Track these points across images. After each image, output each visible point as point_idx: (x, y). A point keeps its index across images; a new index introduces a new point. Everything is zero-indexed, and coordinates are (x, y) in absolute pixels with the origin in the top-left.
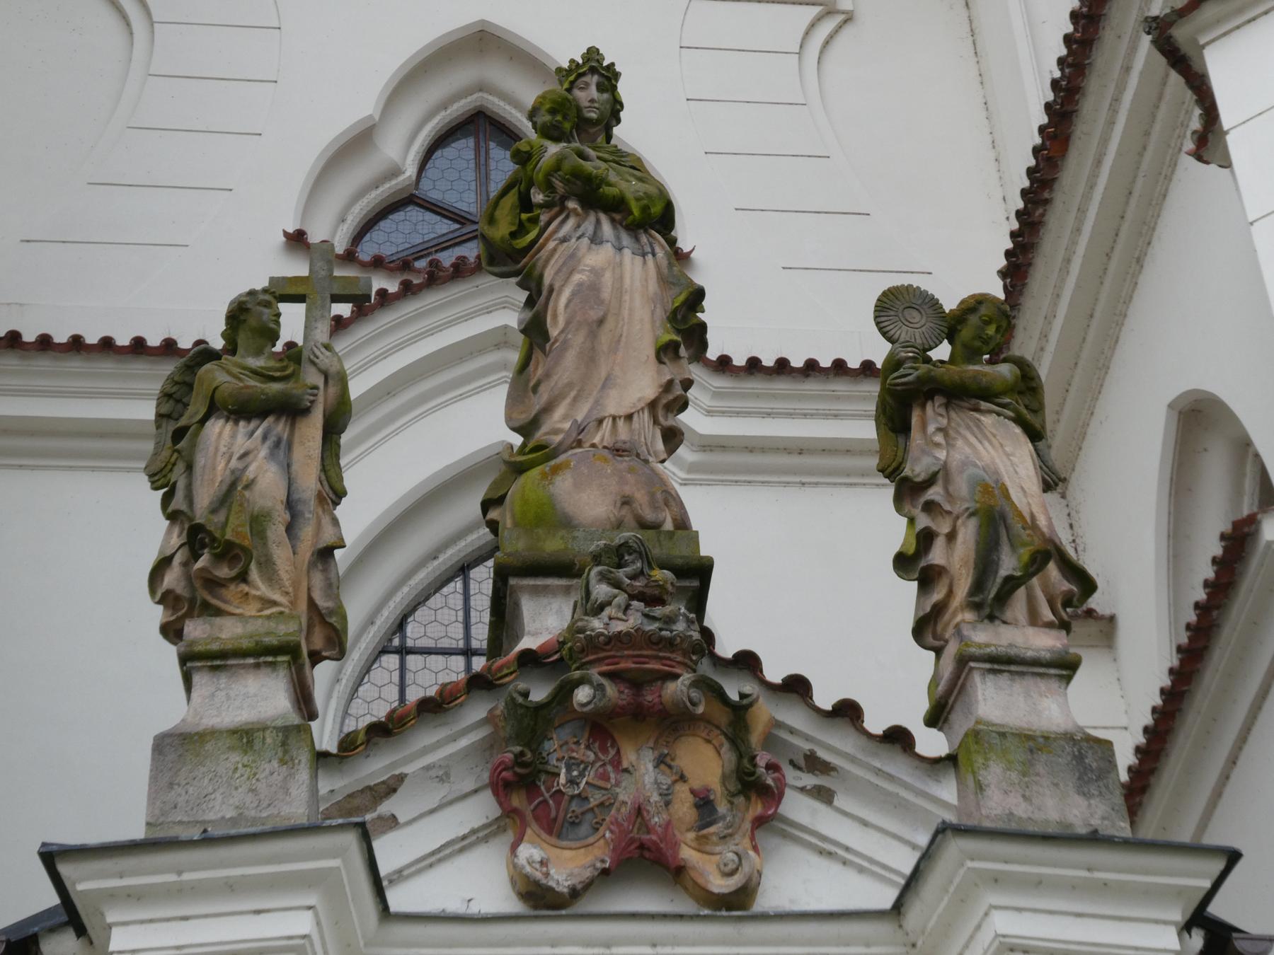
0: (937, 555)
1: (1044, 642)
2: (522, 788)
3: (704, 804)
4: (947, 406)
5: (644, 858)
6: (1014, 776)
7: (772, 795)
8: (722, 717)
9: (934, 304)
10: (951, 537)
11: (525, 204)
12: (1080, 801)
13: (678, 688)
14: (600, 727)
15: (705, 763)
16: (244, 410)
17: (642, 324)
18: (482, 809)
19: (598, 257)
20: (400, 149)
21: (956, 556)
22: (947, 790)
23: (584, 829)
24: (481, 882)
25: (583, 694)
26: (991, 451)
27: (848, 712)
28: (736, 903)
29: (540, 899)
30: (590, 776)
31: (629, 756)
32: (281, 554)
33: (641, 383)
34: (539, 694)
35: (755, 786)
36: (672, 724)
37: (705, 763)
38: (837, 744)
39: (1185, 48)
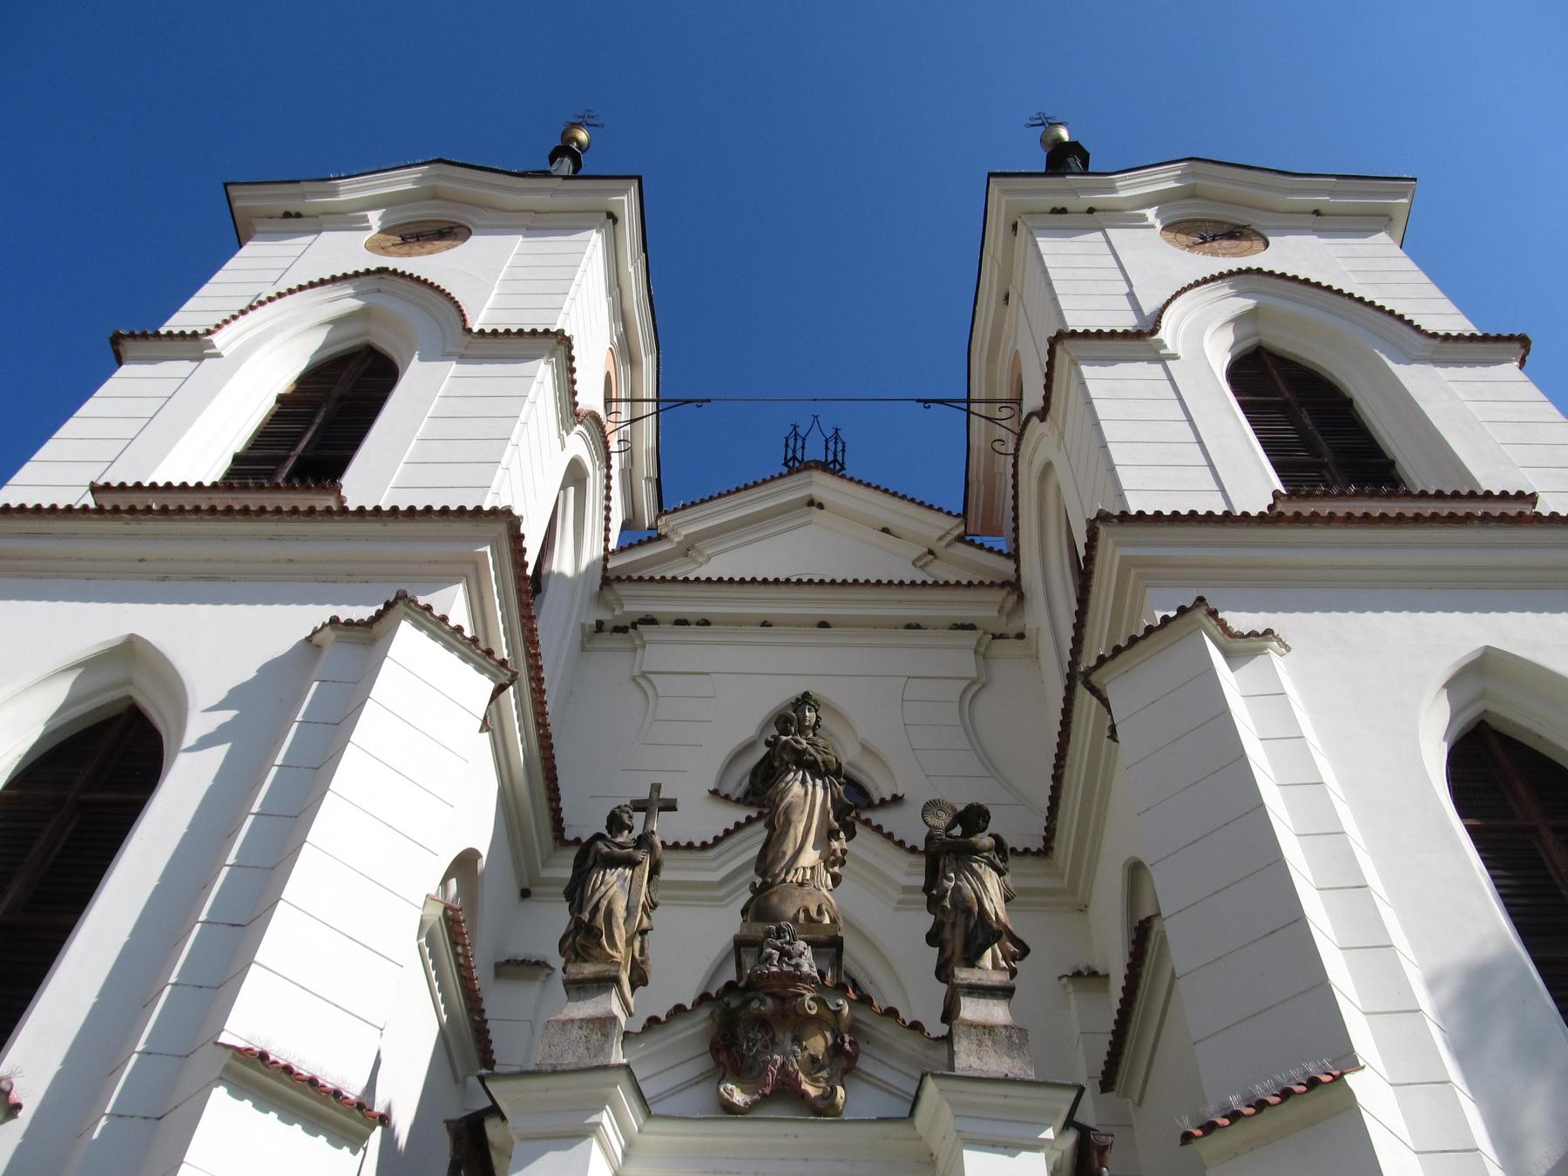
0: (947, 934)
1: (999, 978)
4: (957, 859)
5: (785, 1092)
6: (974, 1047)
7: (852, 1058)
8: (829, 1016)
9: (954, 809)
10: (954, 924)
11: (772, 767)
12: (1006, 1059)
23: (755, 1074)
25: (755, 1004)
27: (892, 1013)
30: (759, 1045)
31: (779, 1036)
32: (620, 935)
34: (734, 1003)
38: (886, 1030)
39: (1098, 686)
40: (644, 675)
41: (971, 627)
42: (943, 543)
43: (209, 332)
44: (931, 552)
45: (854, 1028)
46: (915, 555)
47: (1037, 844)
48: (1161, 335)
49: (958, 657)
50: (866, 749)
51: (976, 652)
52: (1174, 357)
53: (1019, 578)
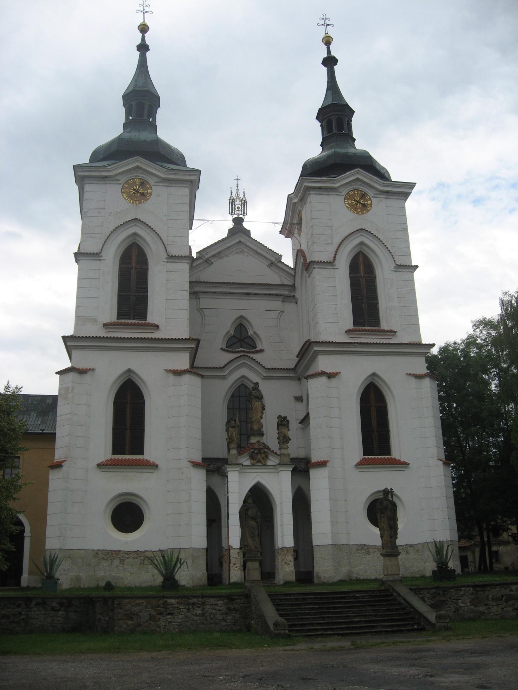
2: (252, 457)
3: (263, 458)
5: (259, 461)
13: (262, 451)
14: (257, 453)
15: (263, 455)
16: (232, 427)
17: (260, 409)
18: (248, 457)
19: (257, 403)
20: (232, 333)
21: (281, 439)
22: (279, 457)
24: (248, 462)
26: (284, 430)
28: (265, 465)
29: (253, 465)
33: (259, 415)
34: (253, 450)
35: (267, 457)
36: (261, 453)
37: (263, 455)
40: (201, 309)
41: (281, 295)
42: (276, 262)
43: (100, 252)
44: (272, 263)
45: (268, 453)
46: (268, 264)
47: (292, 366)
48: (336, 262)
49: (277, 304)
50: (255, 333)
51: (282, 301)
52: (337, 269)
53: (295, 275)
